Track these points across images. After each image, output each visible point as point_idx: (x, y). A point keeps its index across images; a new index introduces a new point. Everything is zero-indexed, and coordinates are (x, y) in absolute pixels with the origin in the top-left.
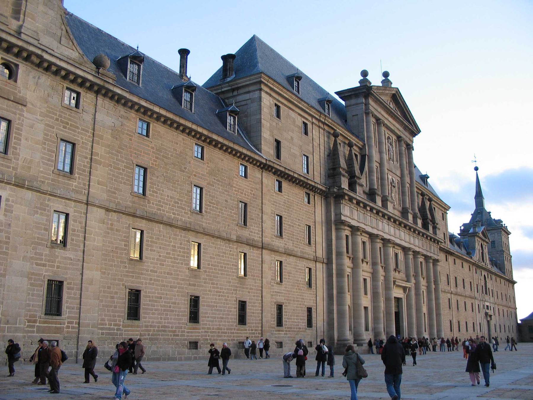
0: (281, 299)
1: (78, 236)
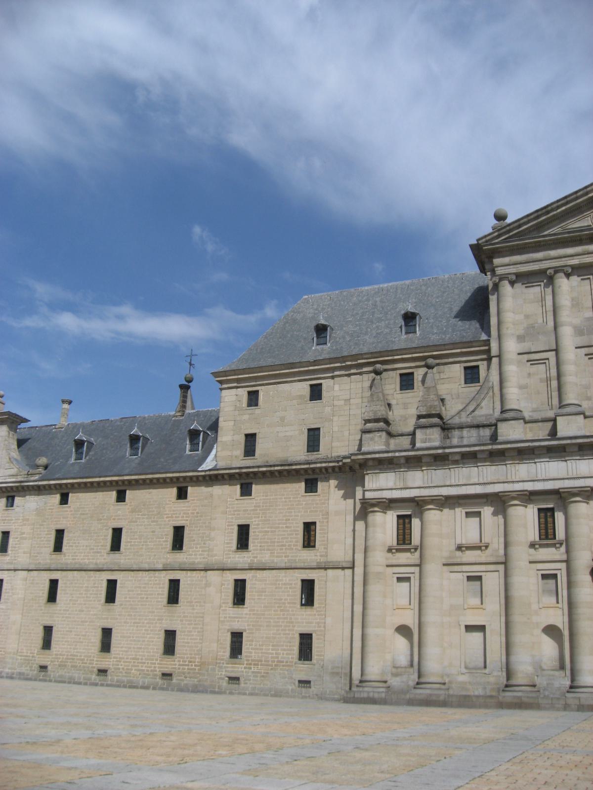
0: (237, 627)
1: (9, 593)
